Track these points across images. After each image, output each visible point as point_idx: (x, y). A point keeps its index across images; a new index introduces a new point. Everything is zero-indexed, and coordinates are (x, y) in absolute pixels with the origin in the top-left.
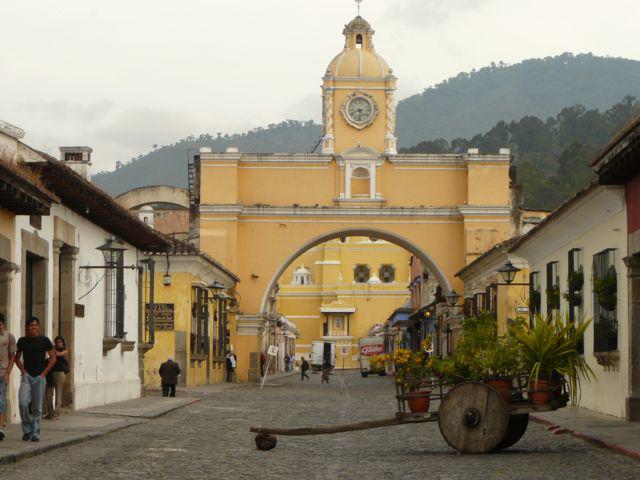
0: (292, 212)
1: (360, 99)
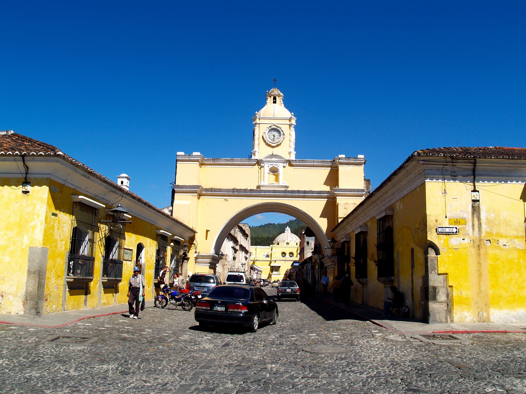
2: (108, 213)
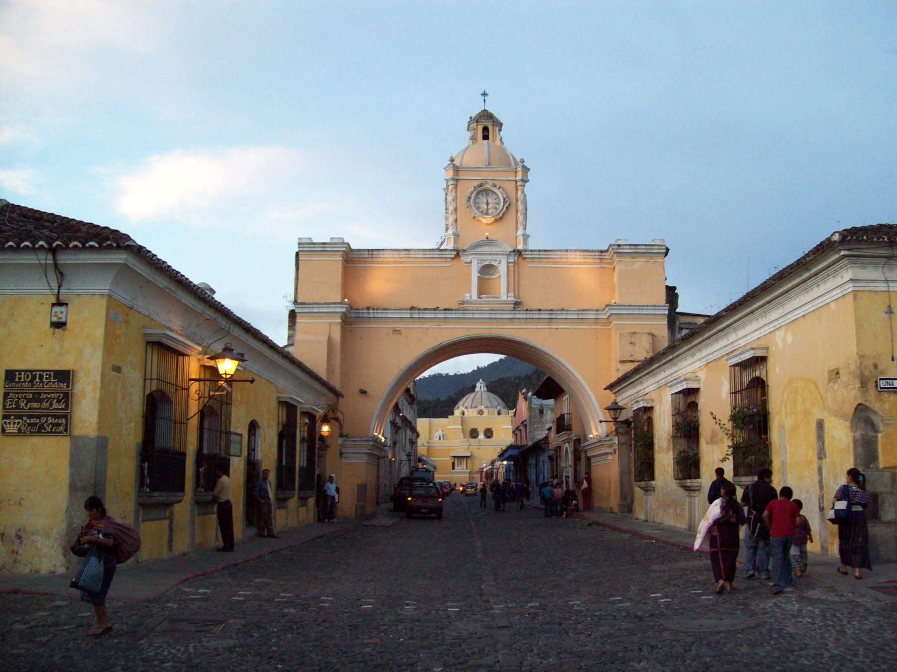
0: (408, 316)
2: (202, 363)
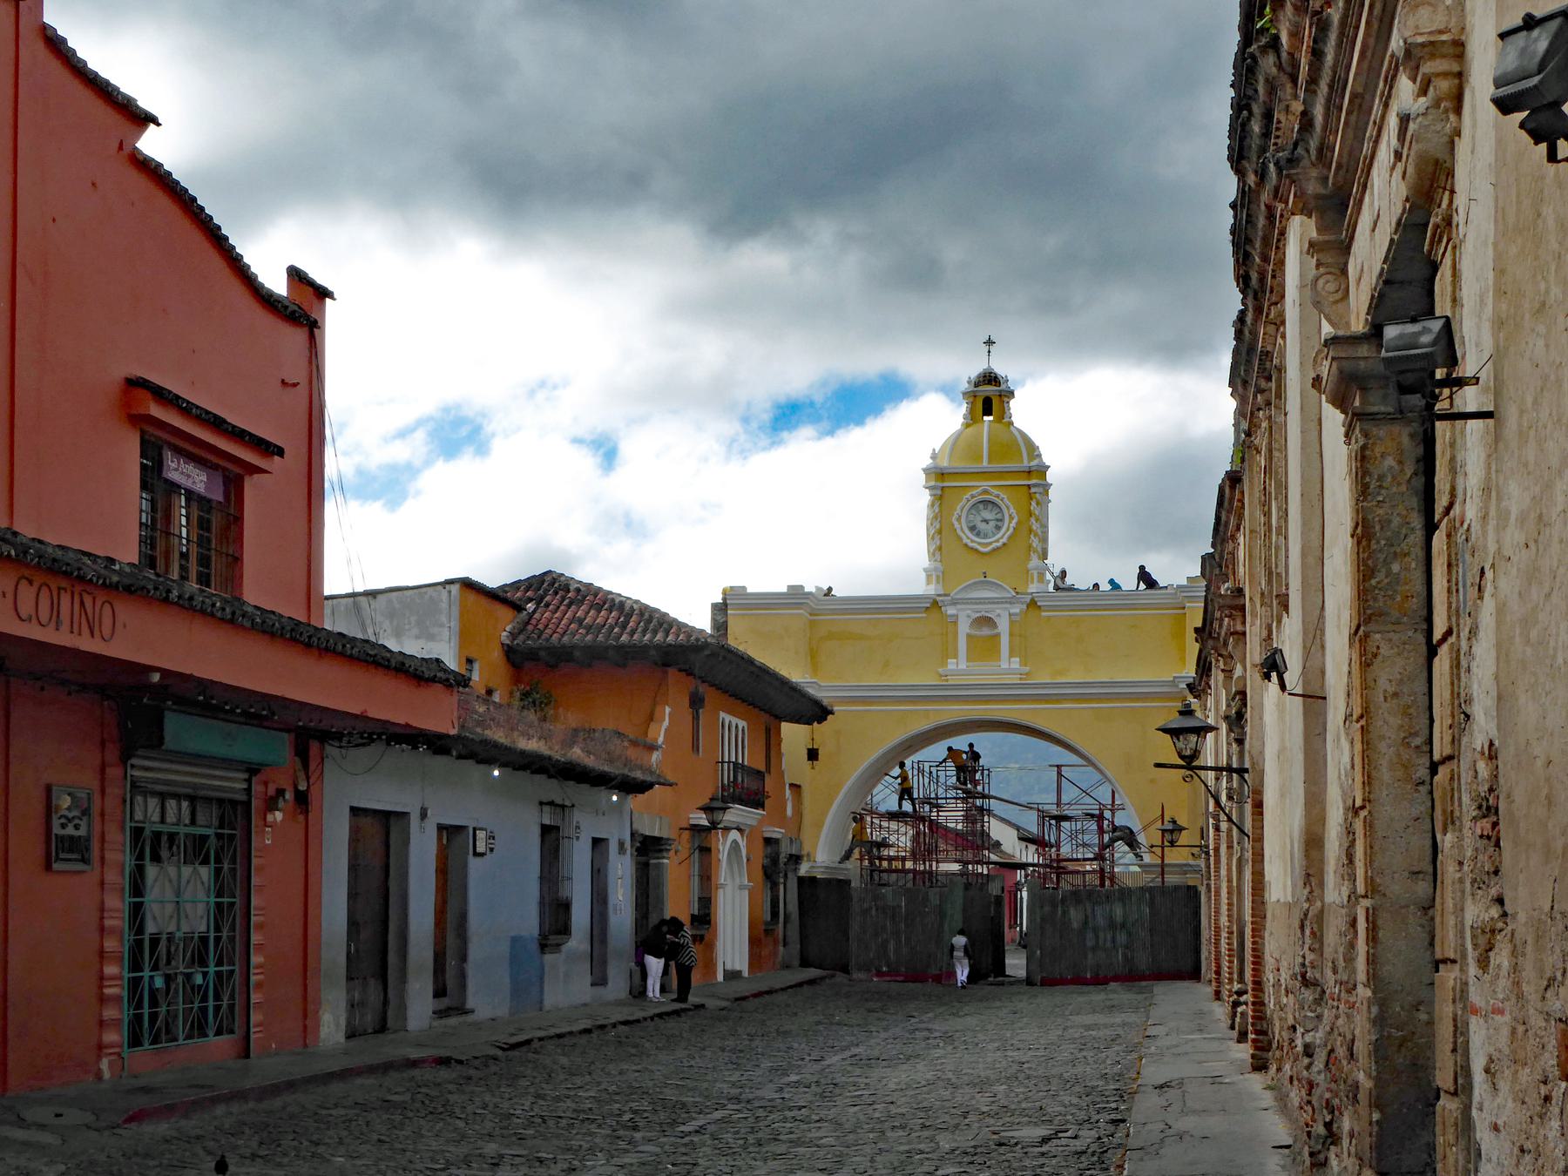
1: (985, 502)
